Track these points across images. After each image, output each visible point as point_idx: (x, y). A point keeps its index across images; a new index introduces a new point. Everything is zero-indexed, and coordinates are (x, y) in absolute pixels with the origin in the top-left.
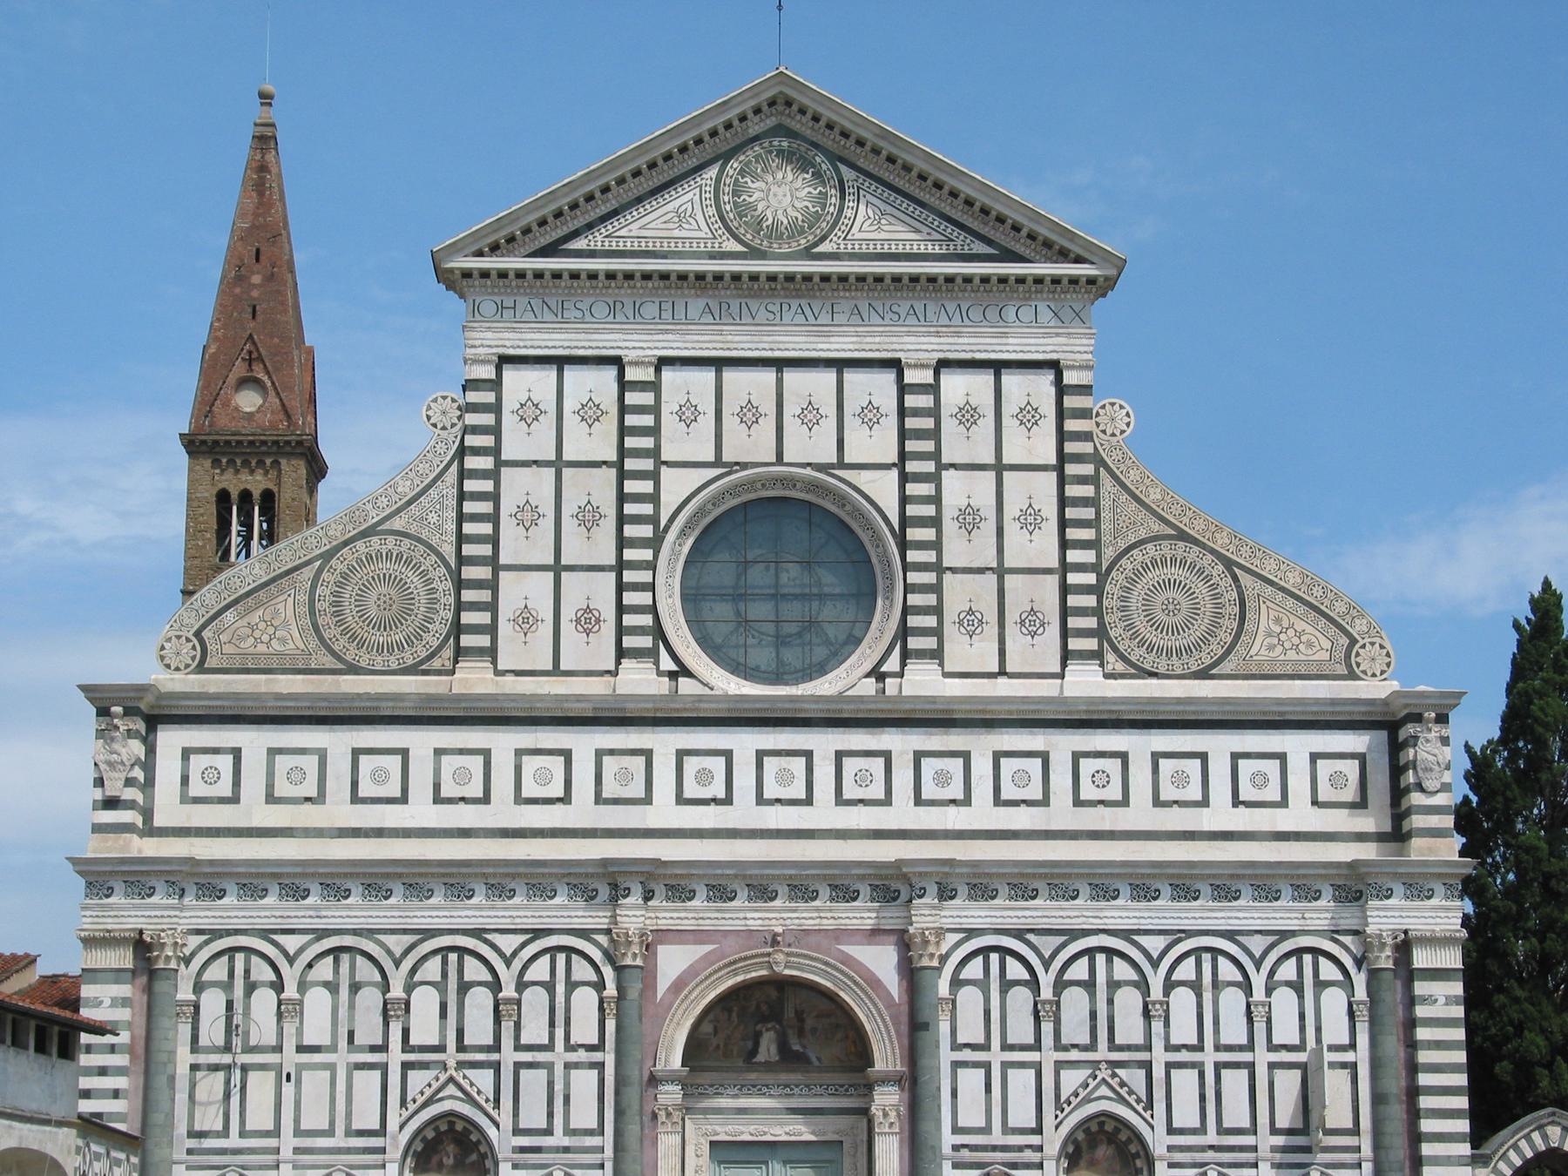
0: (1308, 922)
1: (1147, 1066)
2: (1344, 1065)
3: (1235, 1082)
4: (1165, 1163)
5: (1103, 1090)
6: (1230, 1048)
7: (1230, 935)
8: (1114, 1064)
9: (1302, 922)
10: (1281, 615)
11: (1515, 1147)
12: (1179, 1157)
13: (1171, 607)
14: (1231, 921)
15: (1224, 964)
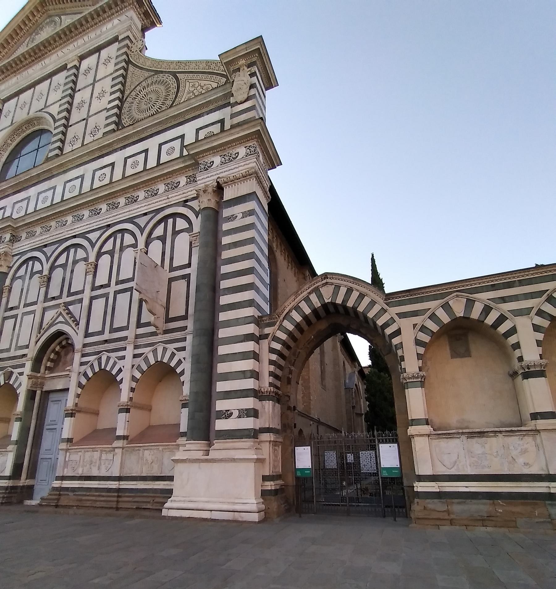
0: (170, 200)
1: (81, 301)
2: (183, 277)
3: (122, 299)
4: (80, 354)
5: (61, 319)
6: (123, 282)
7: (130, 220)
8: (67, 305)
9: (167, 200)
10: (195, 83)
11: (297, 308)
12: (88, 350)
13: (149, 101)
14: (131, 212)
15: (127, 237)
